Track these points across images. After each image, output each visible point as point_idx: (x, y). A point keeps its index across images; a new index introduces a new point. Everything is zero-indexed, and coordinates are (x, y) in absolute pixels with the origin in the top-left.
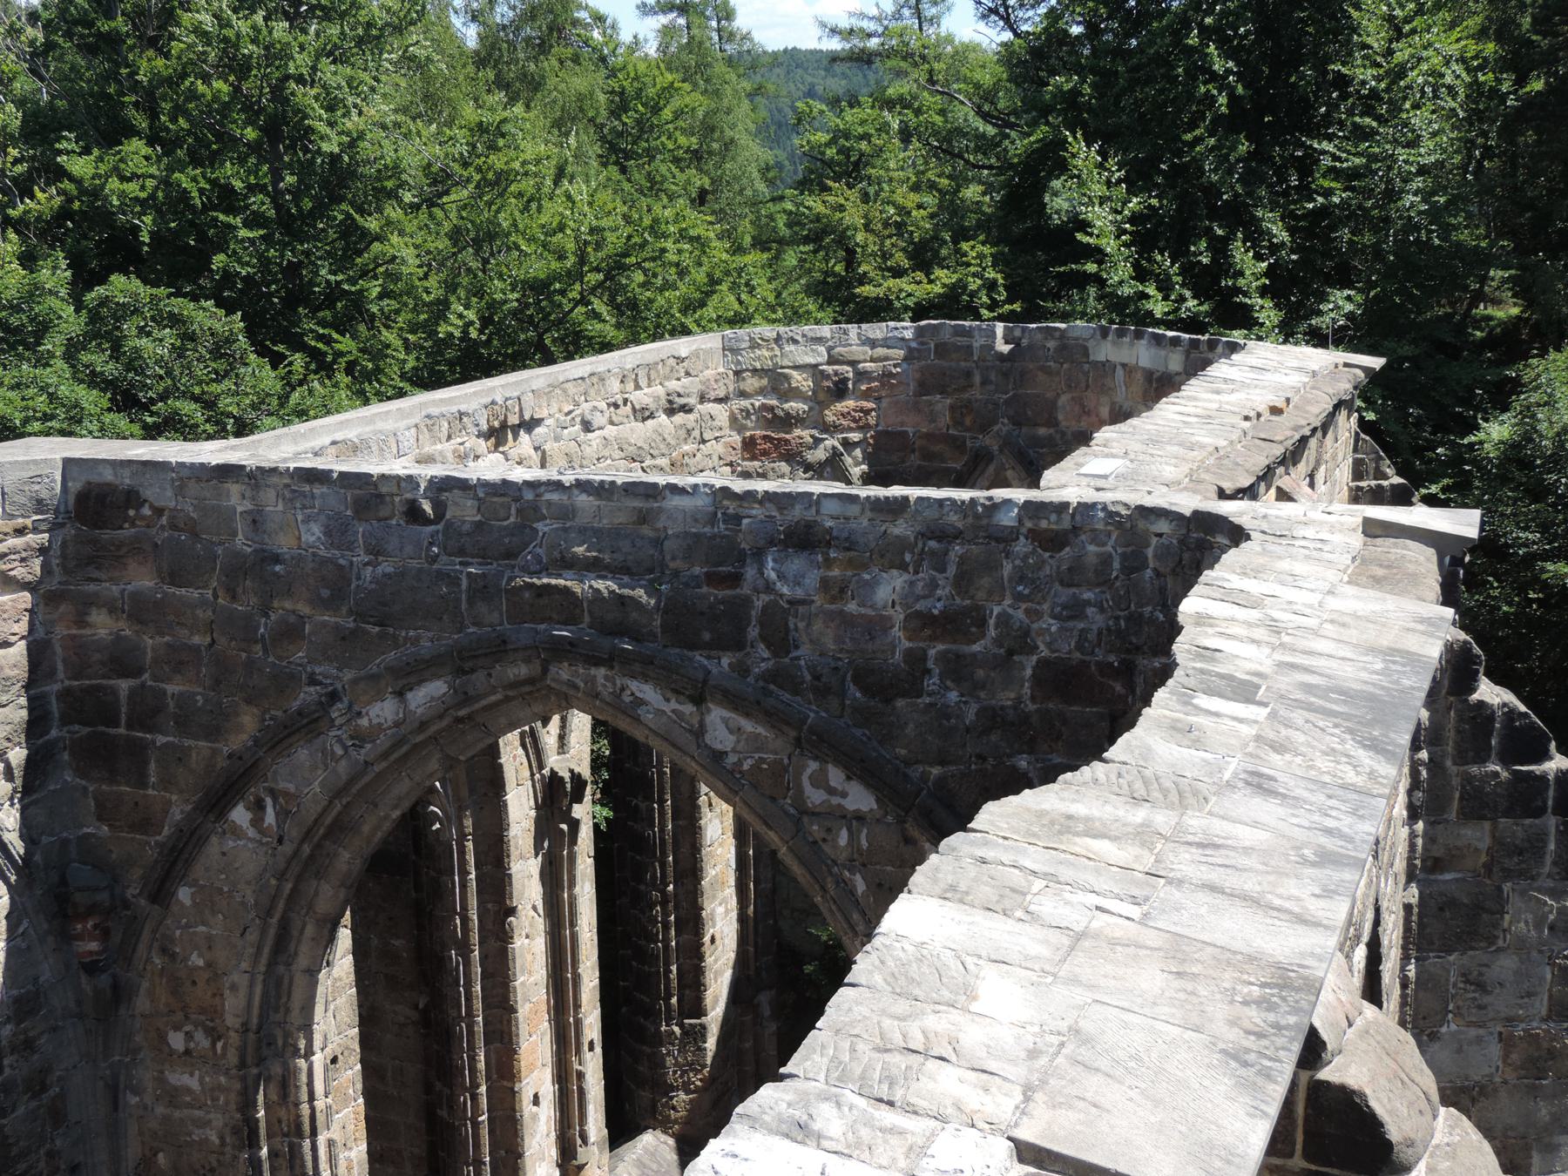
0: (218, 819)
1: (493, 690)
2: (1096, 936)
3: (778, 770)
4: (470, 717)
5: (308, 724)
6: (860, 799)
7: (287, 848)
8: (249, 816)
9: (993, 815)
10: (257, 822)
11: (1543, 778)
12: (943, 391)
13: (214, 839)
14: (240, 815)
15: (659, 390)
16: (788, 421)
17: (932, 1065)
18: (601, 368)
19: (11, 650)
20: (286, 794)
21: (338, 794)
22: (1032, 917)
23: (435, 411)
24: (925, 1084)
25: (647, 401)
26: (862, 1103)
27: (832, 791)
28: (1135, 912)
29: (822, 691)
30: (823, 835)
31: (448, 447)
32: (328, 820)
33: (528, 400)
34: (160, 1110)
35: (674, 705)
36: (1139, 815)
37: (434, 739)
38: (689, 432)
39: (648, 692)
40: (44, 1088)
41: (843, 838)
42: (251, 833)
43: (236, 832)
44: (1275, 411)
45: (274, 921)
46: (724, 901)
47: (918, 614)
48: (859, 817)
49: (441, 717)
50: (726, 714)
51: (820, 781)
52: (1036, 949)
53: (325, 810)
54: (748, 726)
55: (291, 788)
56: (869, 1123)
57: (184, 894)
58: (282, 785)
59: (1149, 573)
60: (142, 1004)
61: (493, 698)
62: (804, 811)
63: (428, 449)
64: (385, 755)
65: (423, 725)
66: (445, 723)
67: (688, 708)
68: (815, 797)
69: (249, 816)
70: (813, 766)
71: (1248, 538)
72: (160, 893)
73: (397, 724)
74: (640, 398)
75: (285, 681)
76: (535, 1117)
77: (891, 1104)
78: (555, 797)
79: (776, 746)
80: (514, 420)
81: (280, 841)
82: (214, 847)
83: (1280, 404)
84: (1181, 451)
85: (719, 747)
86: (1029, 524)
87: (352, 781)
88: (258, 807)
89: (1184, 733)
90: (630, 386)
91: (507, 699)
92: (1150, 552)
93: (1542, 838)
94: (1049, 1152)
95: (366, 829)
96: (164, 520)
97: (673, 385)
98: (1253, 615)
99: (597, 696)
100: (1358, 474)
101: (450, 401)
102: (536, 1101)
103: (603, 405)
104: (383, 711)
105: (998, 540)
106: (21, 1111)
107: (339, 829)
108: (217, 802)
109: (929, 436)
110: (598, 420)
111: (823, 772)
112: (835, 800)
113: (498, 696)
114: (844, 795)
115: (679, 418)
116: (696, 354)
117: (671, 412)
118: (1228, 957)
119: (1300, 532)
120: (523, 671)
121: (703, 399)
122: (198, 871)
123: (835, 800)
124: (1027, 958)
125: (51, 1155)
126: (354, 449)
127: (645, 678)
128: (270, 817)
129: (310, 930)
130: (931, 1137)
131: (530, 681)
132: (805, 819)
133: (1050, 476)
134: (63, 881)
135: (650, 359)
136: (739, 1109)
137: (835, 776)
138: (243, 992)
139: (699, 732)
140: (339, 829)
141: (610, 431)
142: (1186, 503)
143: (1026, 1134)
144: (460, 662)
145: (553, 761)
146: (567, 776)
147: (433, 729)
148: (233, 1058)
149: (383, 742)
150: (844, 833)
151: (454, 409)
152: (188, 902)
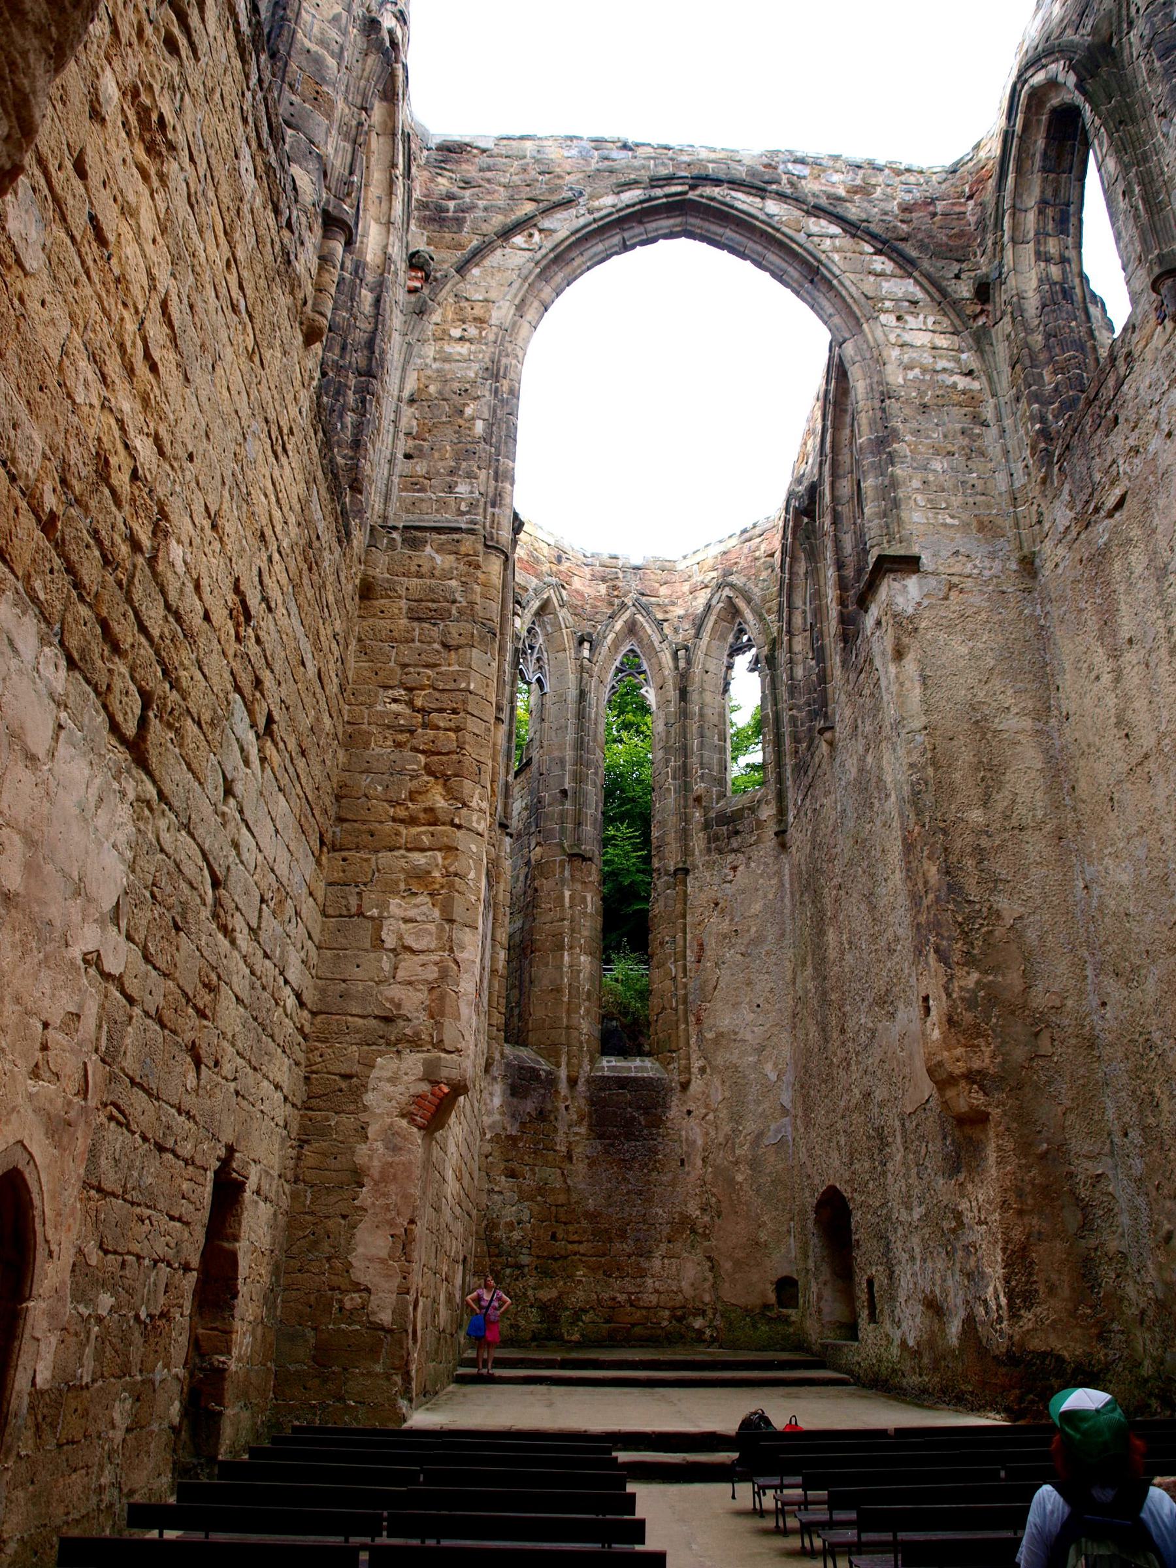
5: (567, 203)
6: (835, 230)
12: (604, 580)
14: (519, 240)
49: (633, 205)
51: (815, 224)
60: (436, 318)
72: (462, 269)
82: (499, 252)
108: (506, 233)
109: (595, 598)
120: (679, 189)
122: (487, 262)
128: (537, 237)
137: (823, 222)
138: (504, 311)
148: (491, 337)
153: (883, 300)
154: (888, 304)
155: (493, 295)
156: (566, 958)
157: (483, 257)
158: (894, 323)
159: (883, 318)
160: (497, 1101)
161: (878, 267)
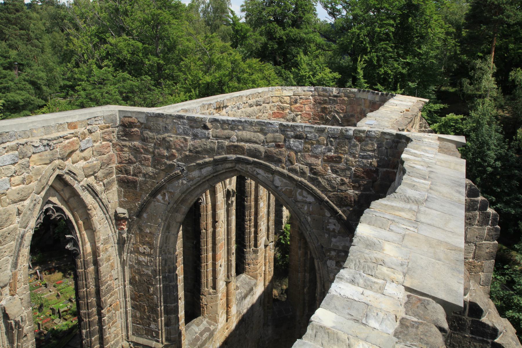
0: (154, 198)
1: (223, 169)
2: (408, 235)
3: (291, 191)
4: (217, 175)
6: (310, 199)
7: (170, 205)
8: (162, 197)
9: (374, 204)
10: (164, 199)
11: (477, 201)
13: (153, 203)
14: (159, 197)
15: (254, 100)
16: (283, 109)
17: (379, 266)
18: (242, 94)
19: (105, 156)
20: (170, 192)
21: (184, 193)
22: (392, 230)
23: (205, 103)
24: (378, 271)
25: (252, 103)
26: (365, 275)
27: (304, 197)
28: (416, 230)
29: (303, 174)
30: (301, 207)
31: (207, 111)
32: (181, 199)
33: (225, 101)
34: (136, 266)
35: (267, 175)
36: (408, 206)
37: (208, 180)
38: (261, 110)
39: (260, 171)
40: (109, 260)
41: (306, 208)
42: (162, 201)
43: (158, 201)
44: (407, 111)
45: (167, 223)
46: (263, 221)
47: (327, 156)
48: (310, 203)
50: (279, 177)
52: (395, 238)
53: (180, 196)
54: (284, 180)
55: (172, 191)
56: (369, 280)
57: (145, 215)
58: (170, 190)
59: (384, 148)
61: (222, 172)
62: (296, 201)
63: (203, 112)
64: (195, 184)
65: (205, 177)
66: (210, 177)
67: (270, 176)
68: (299, 198)
69: (162, 197)
70: (299, 190)
71: (412, 141)
73: (199, 177)
74: (250, 102)
75: (172, 166)
76: (220, 270)
77: (372, 275)
78: (228, 195)
79: (291, 187)
80: (222, 106)
81: (169, 203)
82: (152, 204)
83: (408, 109)
84: (389, 120)
85: (277, 185)
86: (355, 135)
87: (187, 190)
88: (164, 195)
89: (413, 186)
90: (248, 99)
91: (226, 172)
92: (384, 143)
93: (476, 215)
94: (413, 290)
95: (189, 201)
96: (143, 126)
97: (257, 99)
98: (419, 159)
99: (248, 172)
100: (421, 127)
101: (208, 101)
102: (221, 266)
103: (242, 103)
104: (195, 174)
105: (347, 139)
106: (104, 265)
107: (183, 201)
108: (154, 195)
110: (241, 107)
111: (302, 192)
112: (304, 199)
113: (224, 171)
114: (307, 198)
115: (258, 107)
116: (263, 92)
117: (257, 106)
118: (440, 242)
119: (424, 140)
120: (230, 165)
121: (264, 103)
122: (148, 210)
123: (304, 199)
124: (394, 240)
125: (111, 276)
126: (186, 111)
127: (260, 168)
129: (174, 225)
130: (385, 285)
131: (232, 168)
132: (297, 203)
133: (359, 124)
134: (116, 212)
135: (253, 93)
136: (337, 276)
137: (305, 193)
139: (273, 181)
140: (183, 201)
141: (243, 110)
142: (394, 132)
143: (408, 285)
144: (216, 162)
145: (228, 187)
146: (231, 190)
147: (207, 178)
149: (195, 182)
150: (306, 207)
151: (209, 102)
152: (146, 217)
153: (330, 250)
154: (333, 253)
155: (153, 230)
156: (300, 275)
157: (146, 208)
158: (334, 267)
159: (329, 263)
160: (270, 332)
161: (331, 227)
